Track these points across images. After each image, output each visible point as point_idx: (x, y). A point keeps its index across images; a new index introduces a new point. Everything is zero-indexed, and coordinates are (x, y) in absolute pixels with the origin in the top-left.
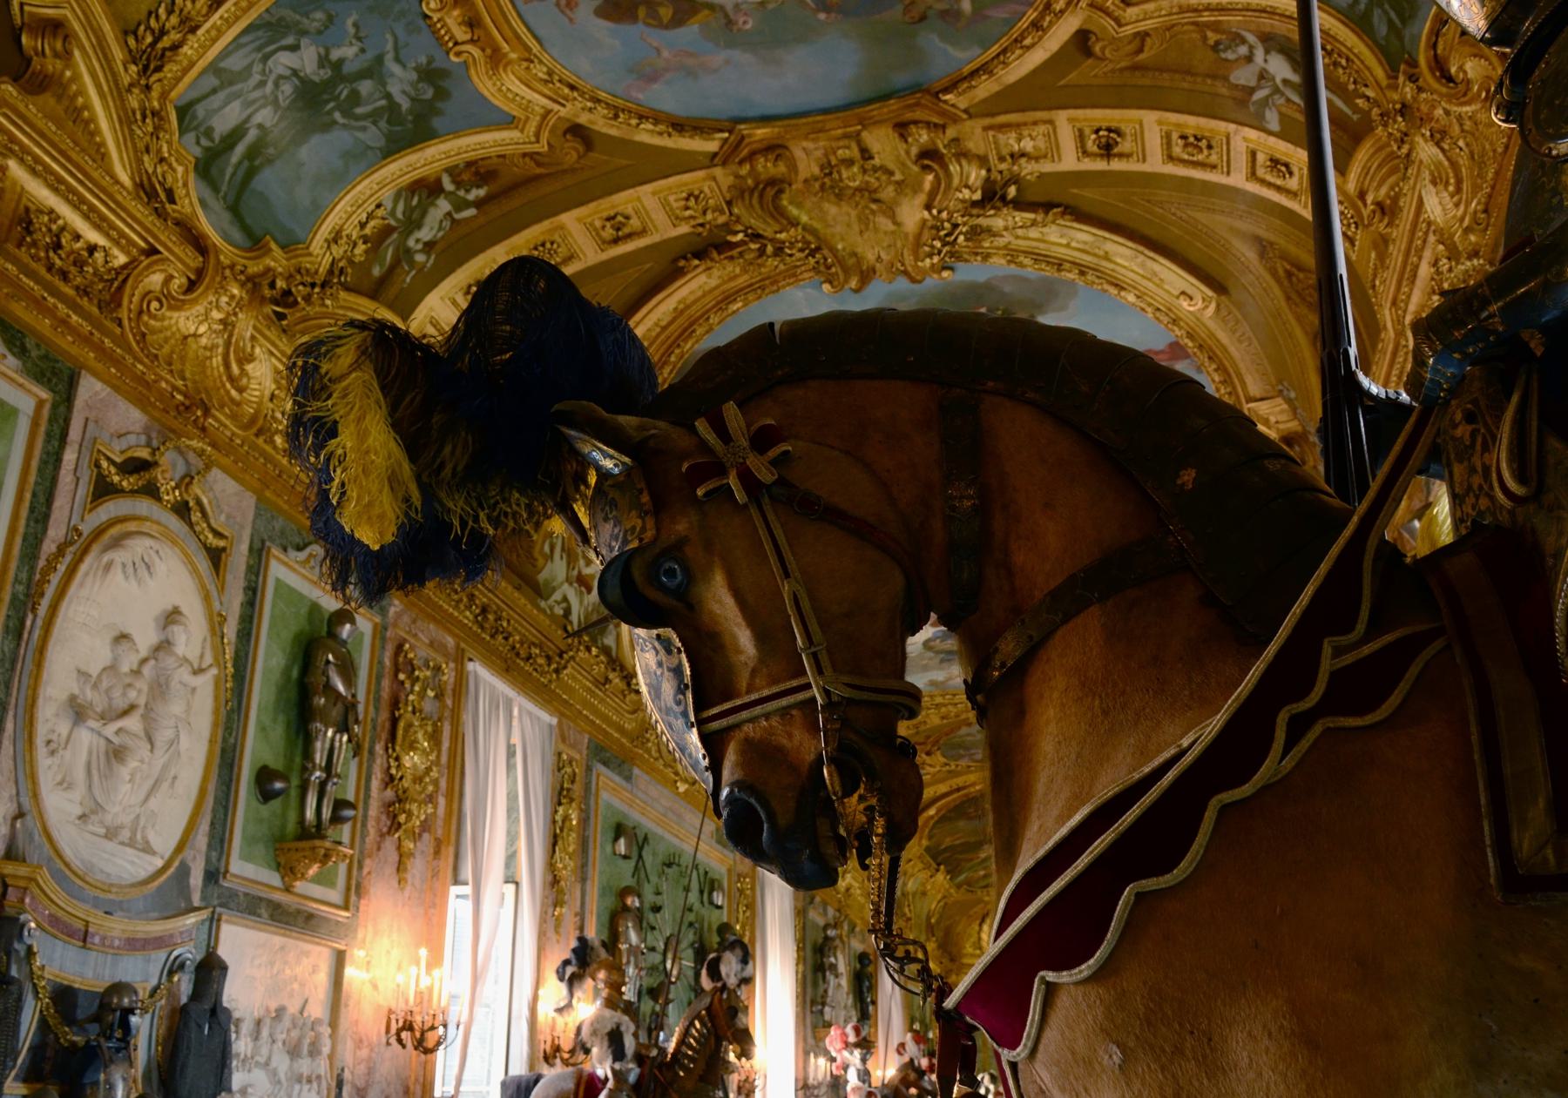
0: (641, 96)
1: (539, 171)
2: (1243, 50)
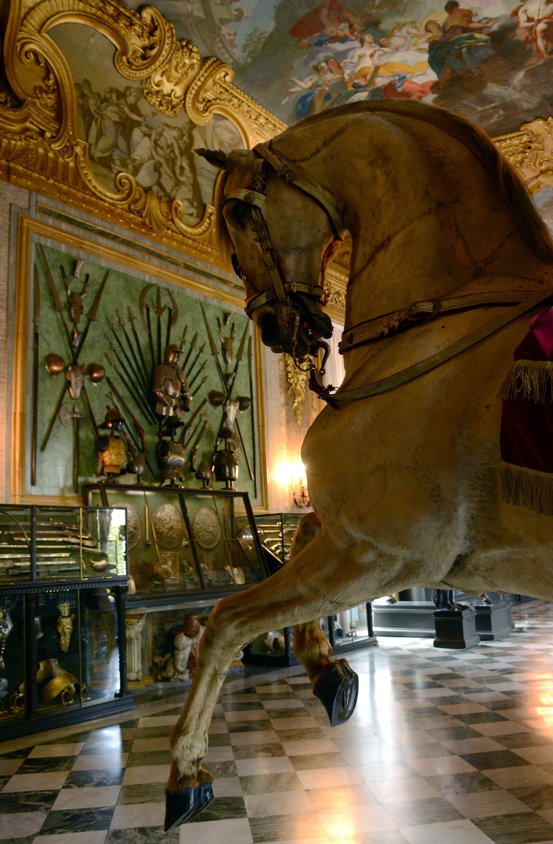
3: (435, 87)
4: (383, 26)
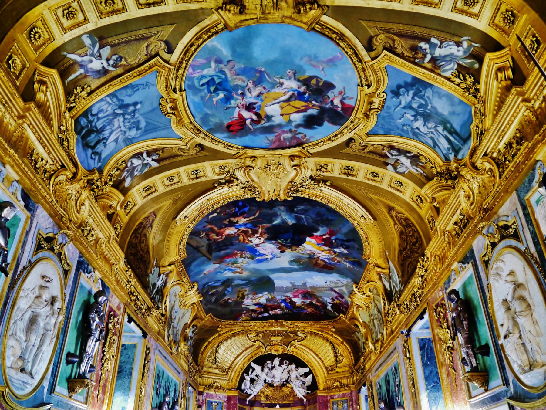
0: (338, 54)
1: (396, 38)
2: (111, 62)
3: (311, 236)
4: (308, 256)
